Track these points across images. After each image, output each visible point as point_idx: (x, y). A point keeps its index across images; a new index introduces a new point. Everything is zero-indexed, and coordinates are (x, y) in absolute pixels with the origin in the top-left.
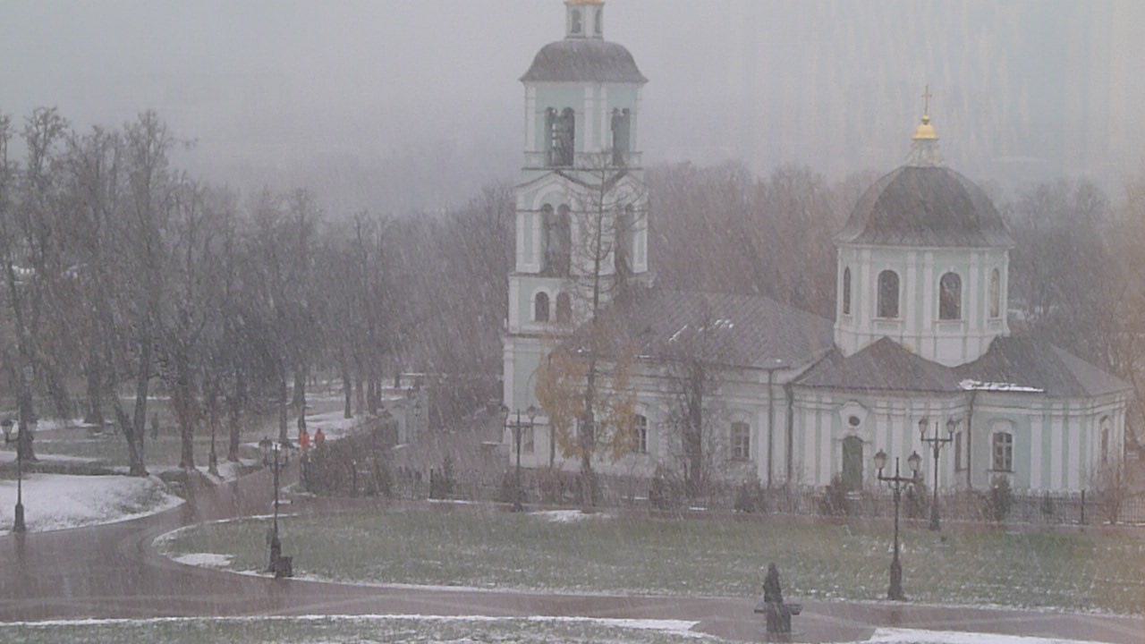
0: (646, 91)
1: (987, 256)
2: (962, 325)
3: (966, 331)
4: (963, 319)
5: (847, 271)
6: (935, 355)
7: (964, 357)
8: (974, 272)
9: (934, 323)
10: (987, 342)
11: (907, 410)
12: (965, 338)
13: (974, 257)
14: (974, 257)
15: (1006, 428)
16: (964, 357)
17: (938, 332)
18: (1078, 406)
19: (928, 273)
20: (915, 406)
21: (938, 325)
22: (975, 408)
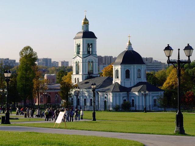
0: (97, 40)
1: (135, 66)
3: (131, 80)
5: (117, 71)
7: (131, 86)
8: (132, 70)
9: (124, 79)
12: (131, 82)
15: (133, 98)
17: (125, 81)
19: (123, 70)
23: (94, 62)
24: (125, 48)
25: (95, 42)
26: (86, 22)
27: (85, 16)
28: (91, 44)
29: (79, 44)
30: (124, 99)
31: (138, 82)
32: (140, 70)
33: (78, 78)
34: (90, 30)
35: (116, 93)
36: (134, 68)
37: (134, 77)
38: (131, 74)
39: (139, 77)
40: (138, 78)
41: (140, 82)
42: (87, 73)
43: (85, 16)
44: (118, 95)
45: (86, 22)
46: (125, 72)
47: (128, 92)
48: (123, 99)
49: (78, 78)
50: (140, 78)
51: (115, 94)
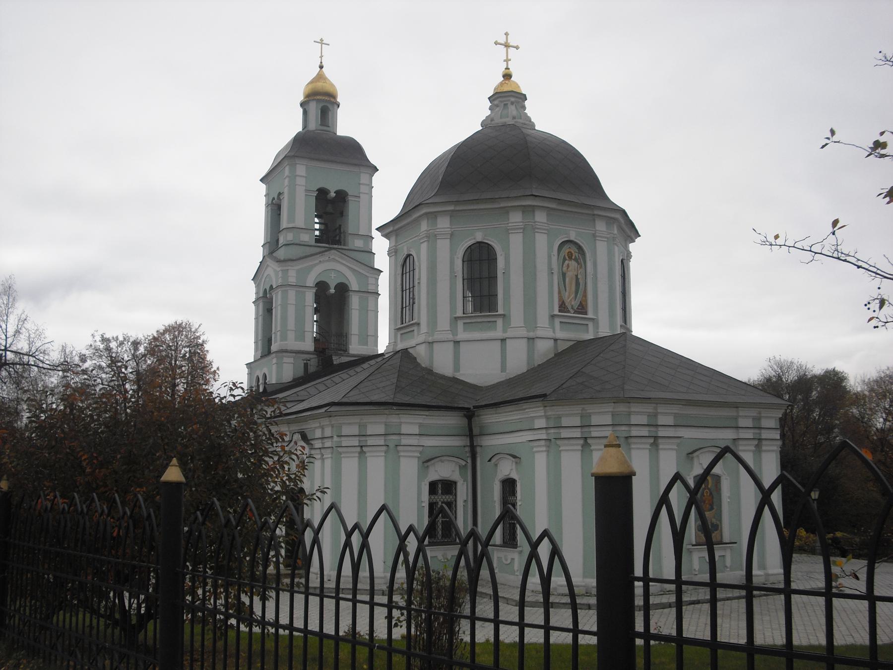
0: (376, 178)
2: (500, 322)
3: (505, 331)
4: (500, 312)
6: (457, 367)
8: (516, 241)
10: (544, 349)
11: (335, 439)
13: (516, 218)
14: (516, 218)
15: (506, 469)
16: (503, 368)
17: (462, 335)
18: (608, 420)
19: (443, 245)
20: (346, 430)
21: (460, 324)
22: (479, 441)
23: (354, 285)
24: (466, 120)
25: (363, 189)
26: (321, 101)
27: (321, 67)
28: (342, 196)
29: (280, 194)
30: (433, 476)
31: (562, 346)
32: (580, 248)
33: (265, 376)
34: (342, 130)
35: (366, 419)
36: (529, 231)
37: (530, 302)
38: (506, 273)
39: (572, 302)
40: (563, 307)
41: (579, 346)
42: (309, 346)
43: (321, 67)
44: (381, 441)
45: (321, 101)
46: (459, 263)
47: (470, 414)
48: (420, 479)
49: (265, 376)
50: (582, 309)
51: (355, 430)
